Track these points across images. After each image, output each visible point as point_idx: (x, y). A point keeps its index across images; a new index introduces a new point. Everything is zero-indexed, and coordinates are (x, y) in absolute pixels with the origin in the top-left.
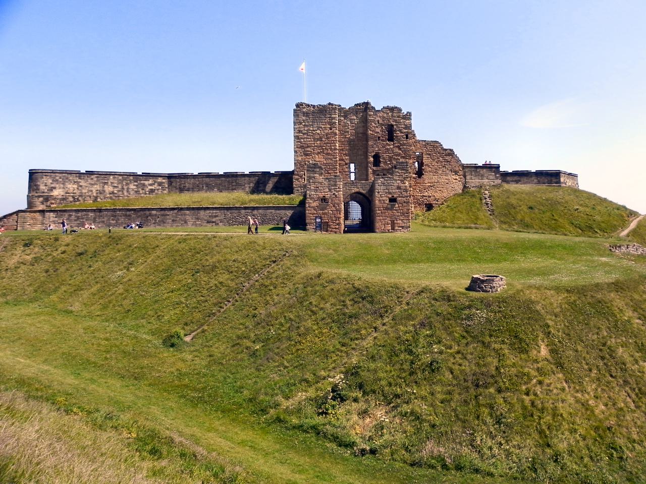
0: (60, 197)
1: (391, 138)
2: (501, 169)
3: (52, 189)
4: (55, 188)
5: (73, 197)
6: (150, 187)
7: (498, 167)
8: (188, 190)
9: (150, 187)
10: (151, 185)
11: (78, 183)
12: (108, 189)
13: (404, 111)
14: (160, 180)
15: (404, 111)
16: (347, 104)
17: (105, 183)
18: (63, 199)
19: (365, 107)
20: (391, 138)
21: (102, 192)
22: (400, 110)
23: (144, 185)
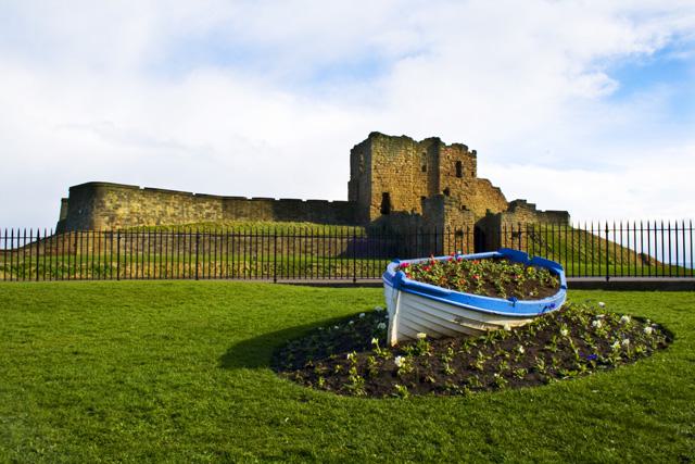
0: (125, 217)
1: (459, 175)
2: (537, 209)
3: (117, 207)
4: (120, 206)
5: (138, 218)
6: (207, 211)
7: (534, 206)
8: (246, 216)
9: (207, 211)
10: (208, 208)
11: (142, 201)
12: (170, 210)
13: (470, 150)
14: (215, 203)
15: (470, 150)
16: (418, 138)
17: (167, 204)
18: (128, 220)
19: (435, 143)
20: (459, 175)
21: (163, 214)
22: (466, 148)
23: (201, 207)
